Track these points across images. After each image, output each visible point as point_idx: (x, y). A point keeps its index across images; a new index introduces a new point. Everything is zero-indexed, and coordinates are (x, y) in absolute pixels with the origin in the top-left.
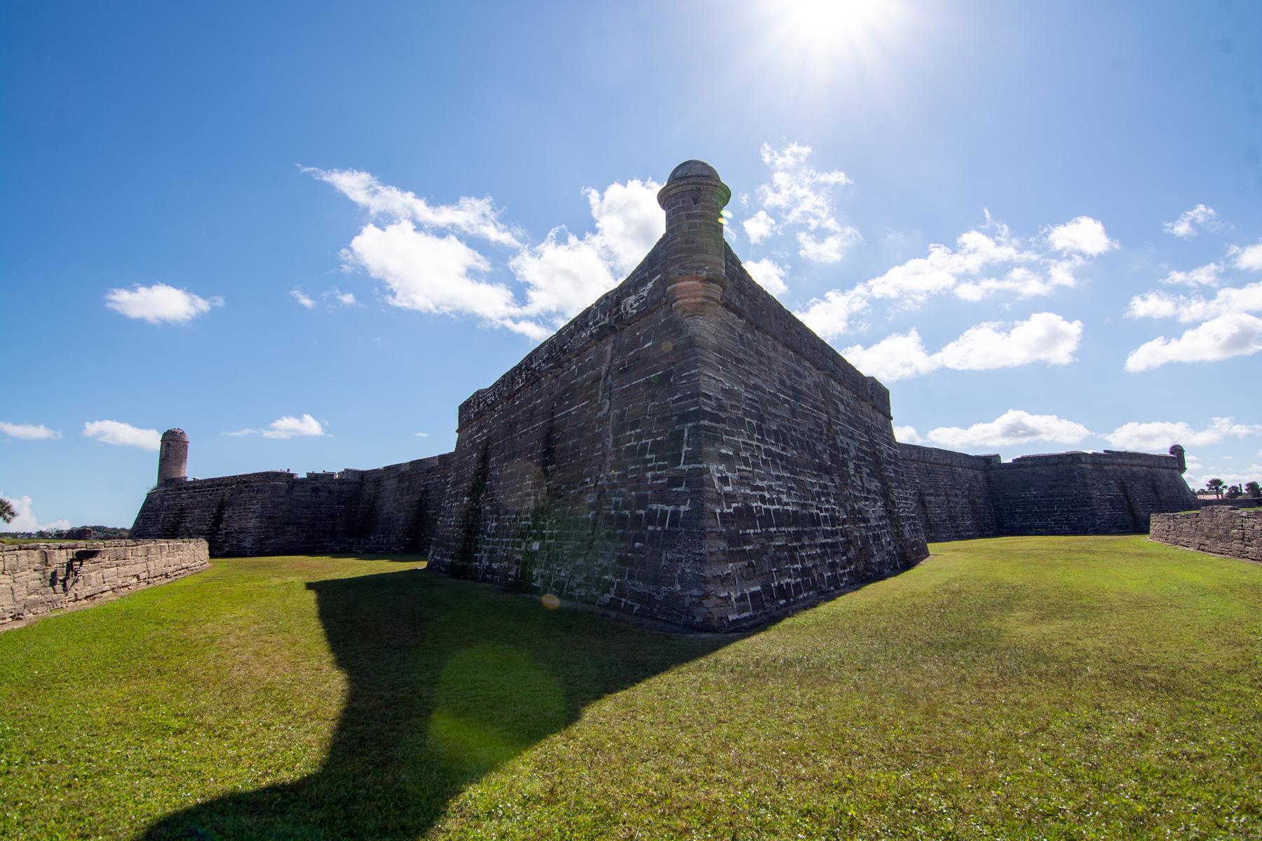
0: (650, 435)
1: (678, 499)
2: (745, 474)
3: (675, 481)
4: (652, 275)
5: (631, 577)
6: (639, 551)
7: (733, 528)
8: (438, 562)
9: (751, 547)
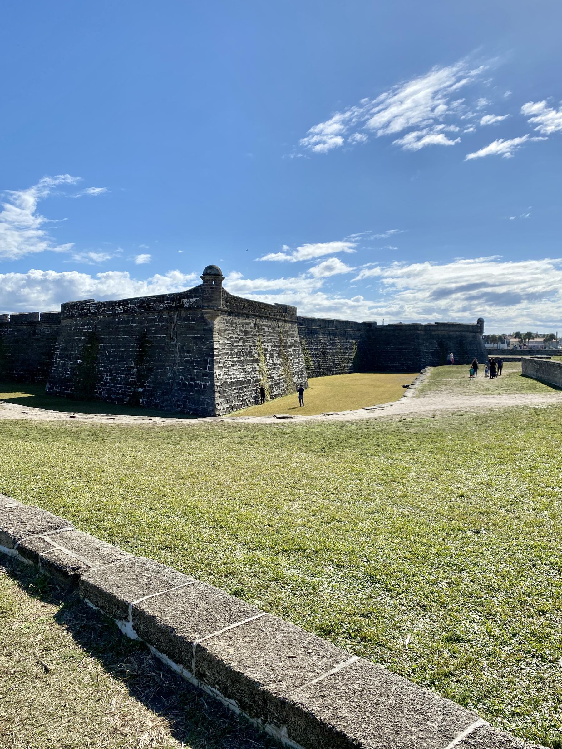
0: (195, 358)
1: (206, 381)
3: (205, 375)
5: (189, 403)
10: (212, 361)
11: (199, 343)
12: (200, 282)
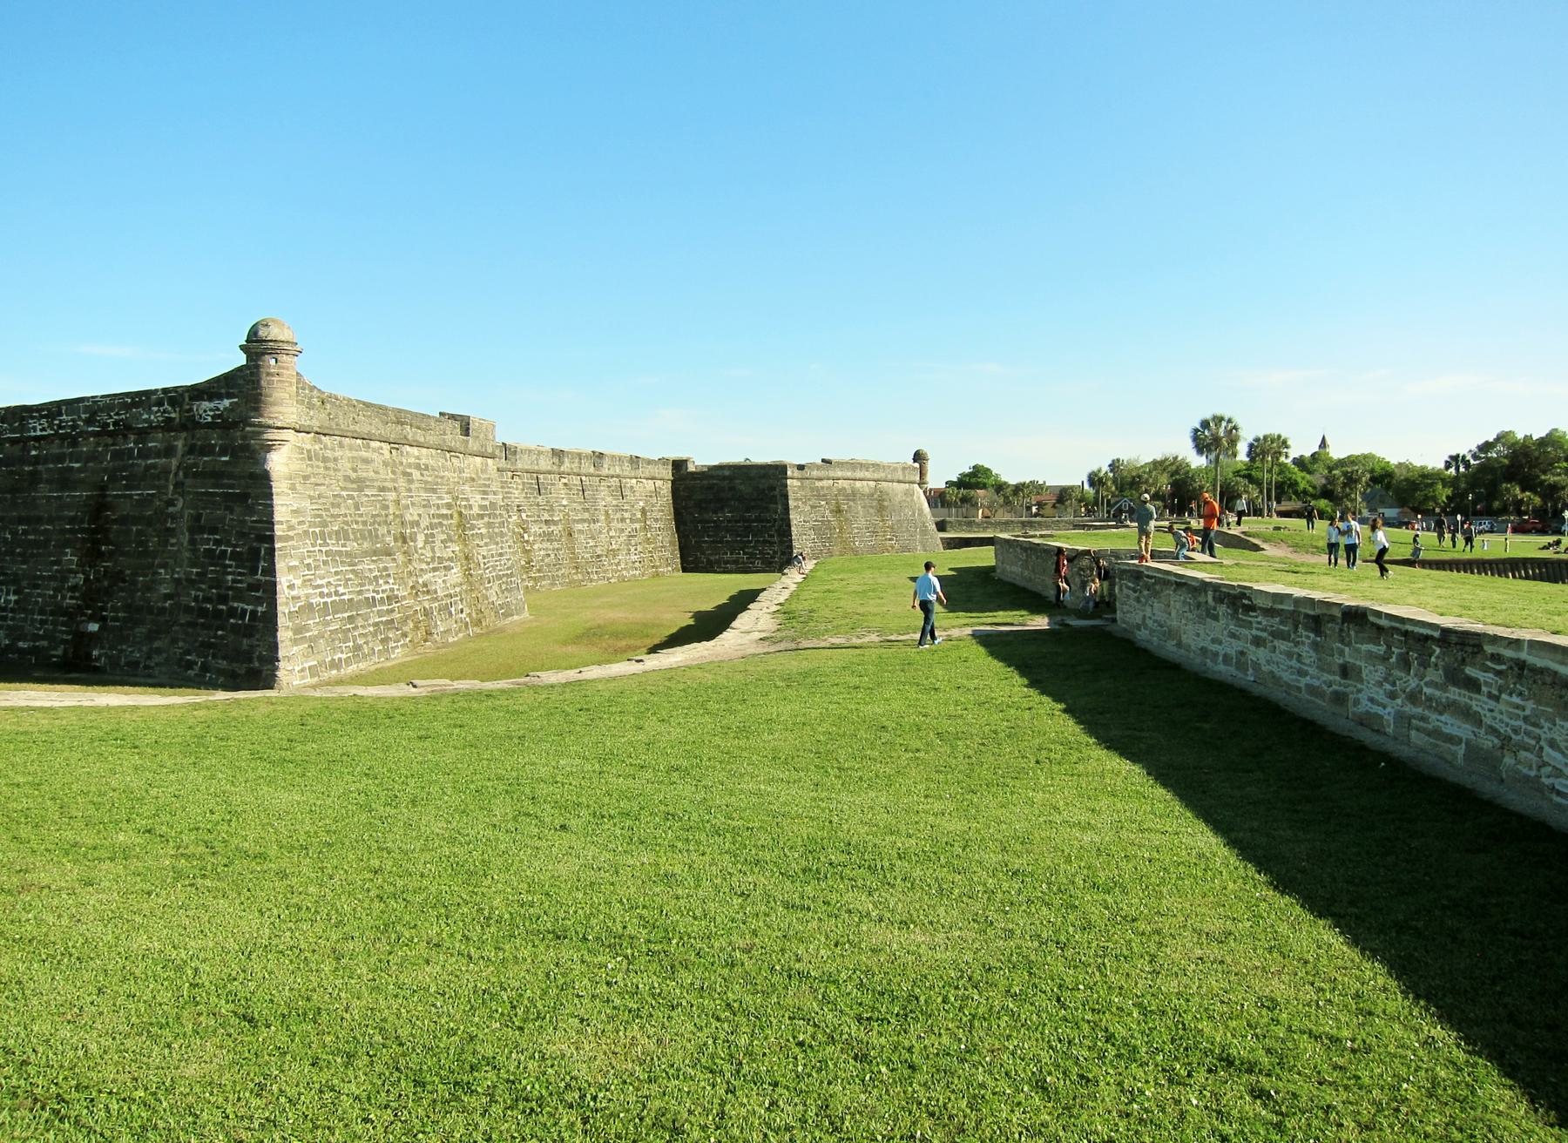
0: (228, 544)
1: (259, 601)
3: (254, 587)
6: (222, 637)
10: (272, 551)
11: (237, 509)
12: (241, 359)
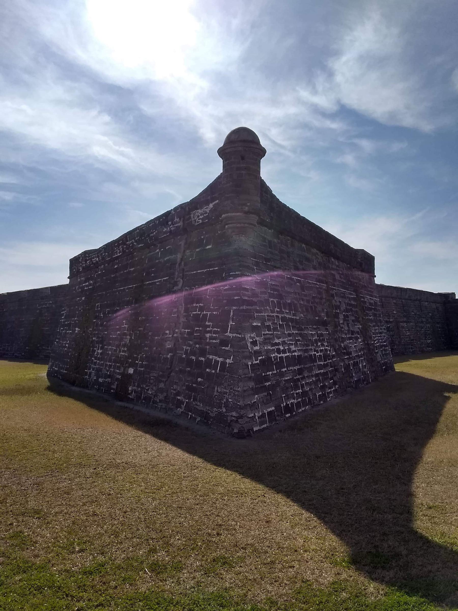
1: (226, 355)
2: (268, 336)
3: (224, 342)
4: (213, 200)
5: (195, 400)
6: (200, 383)
7: (258, 373)
8: (56, 372)
9: (269, 383)
